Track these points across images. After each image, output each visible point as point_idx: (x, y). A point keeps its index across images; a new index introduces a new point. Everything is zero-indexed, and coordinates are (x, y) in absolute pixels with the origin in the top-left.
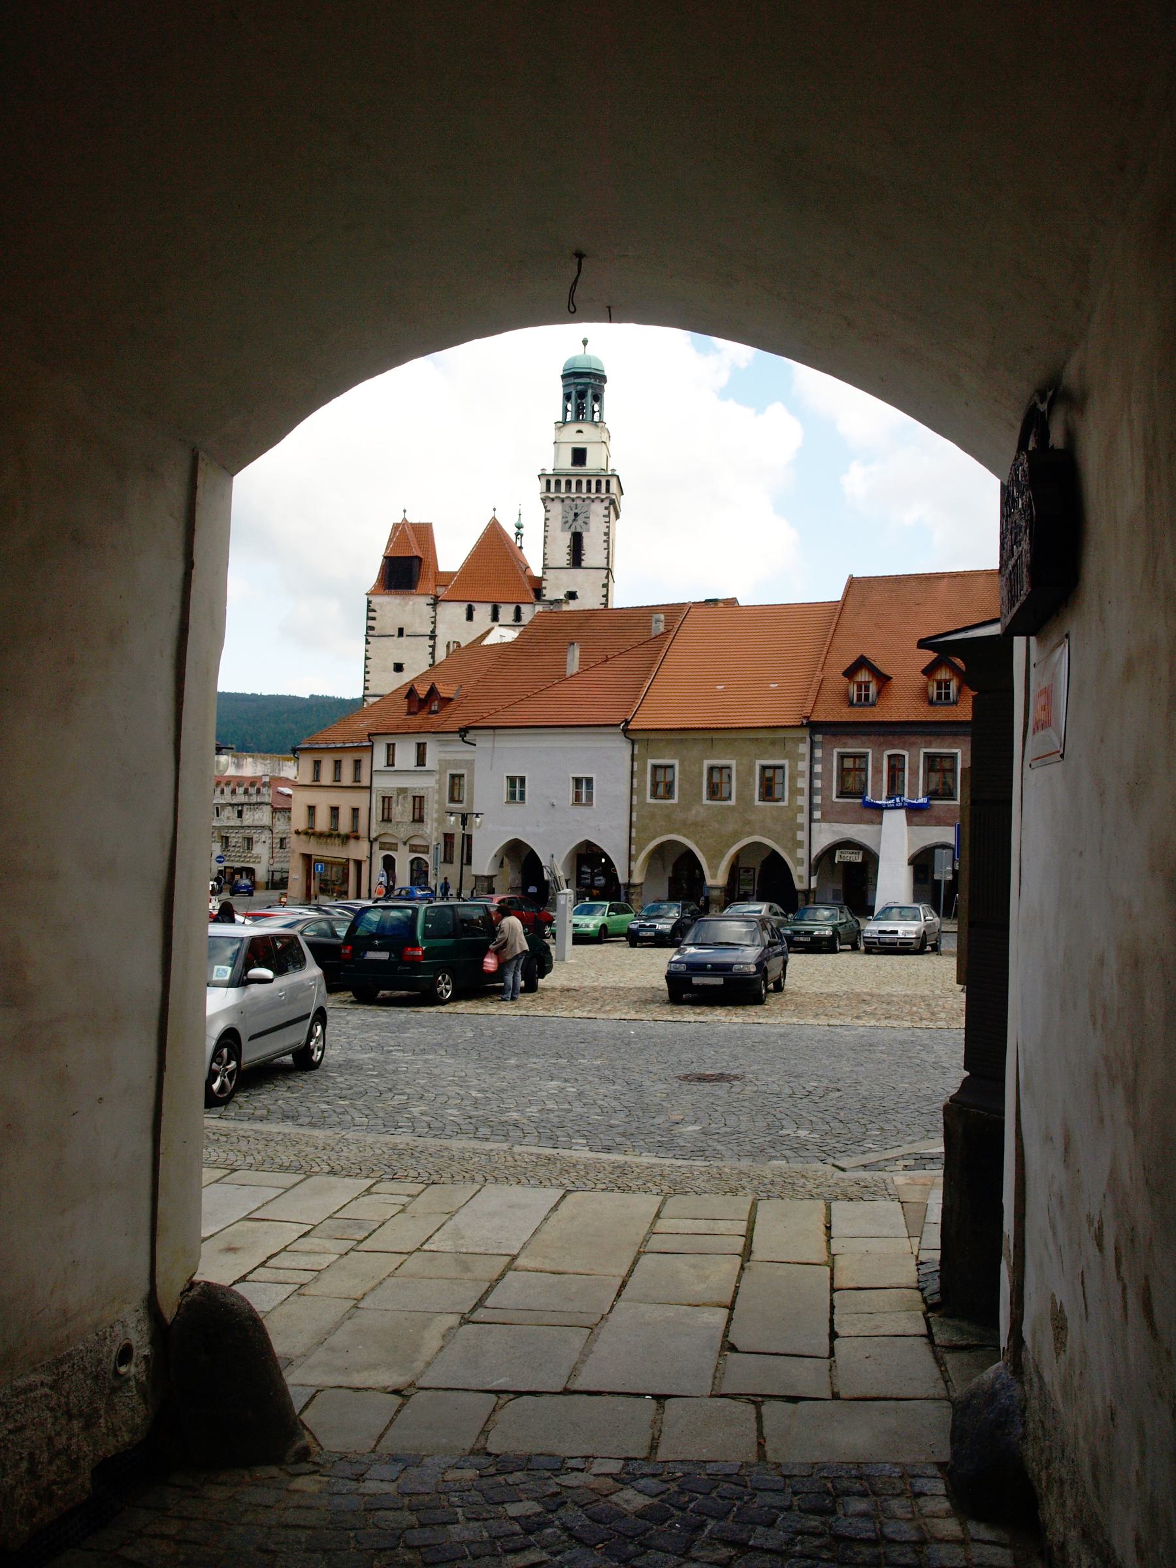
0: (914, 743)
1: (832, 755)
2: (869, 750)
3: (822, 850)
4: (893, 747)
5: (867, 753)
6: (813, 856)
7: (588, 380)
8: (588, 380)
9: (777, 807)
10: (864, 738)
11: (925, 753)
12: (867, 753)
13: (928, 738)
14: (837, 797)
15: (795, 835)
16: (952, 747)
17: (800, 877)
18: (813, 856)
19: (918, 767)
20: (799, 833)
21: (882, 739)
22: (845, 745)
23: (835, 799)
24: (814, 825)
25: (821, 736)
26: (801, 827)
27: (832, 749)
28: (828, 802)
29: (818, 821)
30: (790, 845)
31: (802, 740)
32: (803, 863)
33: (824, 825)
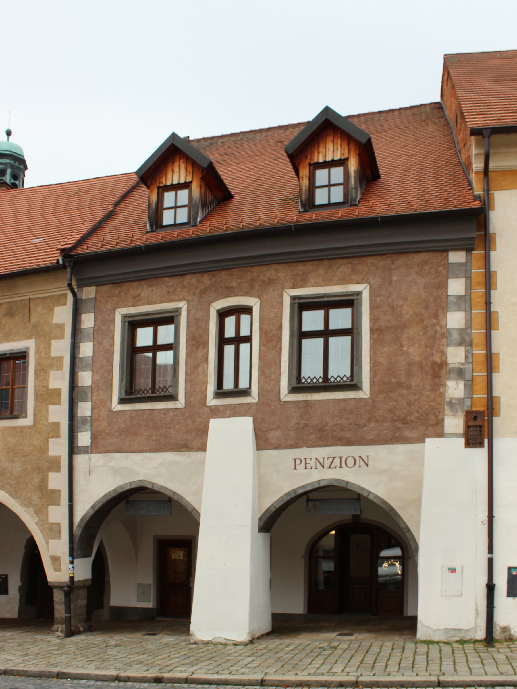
0: (271, 282)
1: (113, 321)
2: (183, 305)
3: (93, 507)
4: (230, 292)
5: (178, 311)
6: (77, 519)
7: (8, 161)
8: (8, 161)
9: (15, 428)
10: (172, 282)
11: (293, 298)
12: (178, 311)
13: (300, 268)
14: (122, 401)
15: (44, 480)
16: (350, 282)
17: (55, 559)
18: (77, 519)
19: (280, 327)
20: (52, 476)
21: (206, 280)
22: (137, 301)
23: (116, 406)
24: (80, 460)
25: (93, 289)
26: (55, 466)
27: (114, 310)
28: (104, 413)
29: (86, 450)
30: (35, 498)
31: (60, 300)
32: (60, 532)
33: (97, 458)
